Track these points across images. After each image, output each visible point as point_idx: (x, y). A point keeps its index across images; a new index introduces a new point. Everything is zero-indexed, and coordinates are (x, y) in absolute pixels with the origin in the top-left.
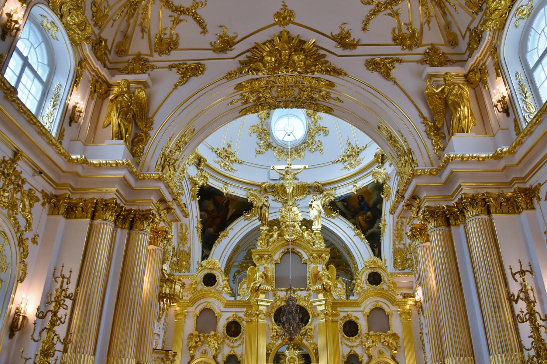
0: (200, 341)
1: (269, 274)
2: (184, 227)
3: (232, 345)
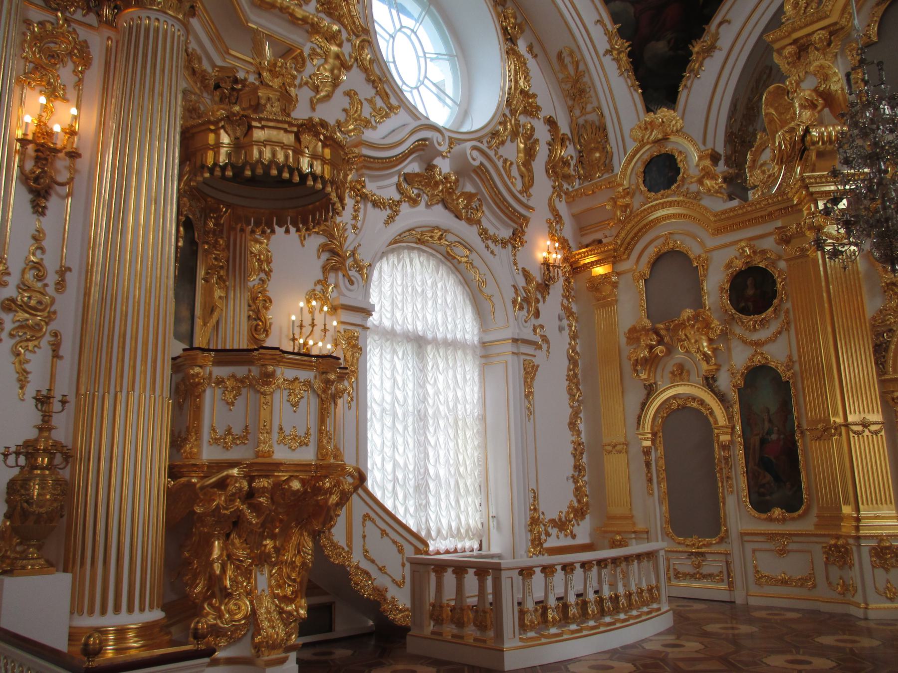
0: (660, 342)
1: (837, 85)
2: (567, 60)
3: (755, 337)
